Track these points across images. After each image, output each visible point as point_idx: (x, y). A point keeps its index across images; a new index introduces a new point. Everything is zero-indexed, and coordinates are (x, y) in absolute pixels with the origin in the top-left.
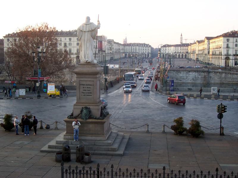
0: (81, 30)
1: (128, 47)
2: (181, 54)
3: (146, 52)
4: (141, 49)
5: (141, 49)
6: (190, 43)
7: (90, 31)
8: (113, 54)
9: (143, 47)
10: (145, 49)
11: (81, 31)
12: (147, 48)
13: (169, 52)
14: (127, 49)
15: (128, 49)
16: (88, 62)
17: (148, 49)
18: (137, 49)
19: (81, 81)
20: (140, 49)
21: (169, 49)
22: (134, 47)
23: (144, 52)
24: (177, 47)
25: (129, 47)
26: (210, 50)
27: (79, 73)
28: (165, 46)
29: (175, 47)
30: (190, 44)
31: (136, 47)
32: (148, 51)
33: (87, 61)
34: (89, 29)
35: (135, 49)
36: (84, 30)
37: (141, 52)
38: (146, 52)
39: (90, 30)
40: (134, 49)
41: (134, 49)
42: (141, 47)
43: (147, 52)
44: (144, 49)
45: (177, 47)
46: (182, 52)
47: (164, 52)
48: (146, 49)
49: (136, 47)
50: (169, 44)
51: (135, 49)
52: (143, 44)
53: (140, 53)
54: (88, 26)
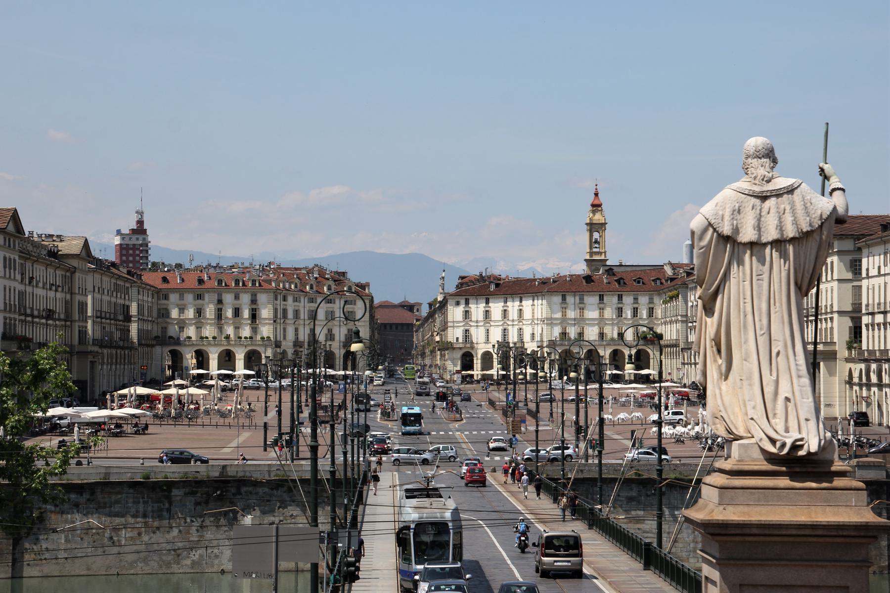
0: (726, 230)
2: (605, 353)
3: (330, 336)
4: (296, 313)
5: (296, 313)
6: (674, 266)
7: (792, 240)
8: (83, 354)
9: (312, 300)
10: (321, 315)
11: (725, 239)
12: (337, 307)
13: (513, 338)
16: (802, 453)
19: (755, 586)
20: (285, 311)
21: (513, 313)
22: (237, 297)
24: (570, 299)
26: (865, 320)
27: (747, 531)
28: (481, 287)
29: (557, 299)
30: (669, 271)
33: (795, 447)
34: (781, 228)
36: (747, 235)
37: (291, 336)
38: (330, 336)
39: (790, 232)
42: (290, 299)
43: (340, 333)
44: (313, 316)
45: (570, 299)
46: (612, 332)
47: (478, 335)
48: (330, 316)
50: (504, 269)
52: (310, 271)
53: (288, 346)
54: (772, 202)
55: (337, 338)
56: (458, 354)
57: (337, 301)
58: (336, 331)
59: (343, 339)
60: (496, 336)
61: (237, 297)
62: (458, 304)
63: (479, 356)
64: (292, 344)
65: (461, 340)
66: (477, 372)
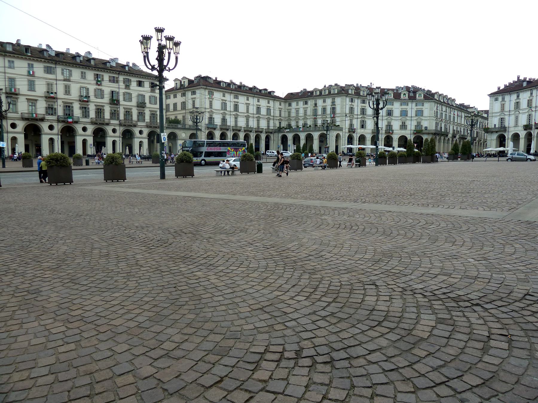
1: (301, 103)
10: (397, 113)
14: (297, 111)
15: (301, 112)
17: (419, 113)
18: (338, 110)
22: (324, 101)
23: (396, 125)
25: (306, 103)
31: (333, 103)
32: (419, 124)
35: (328, 111)
38: (403, 126)
40: (324, 109)
41: (324, 109)
43: (411, 125)
47: (510, 122)
49: (333, 103)
51: (328, 111)
55: (409, 127)
56: (495, 136)
57: (410, 104)
58: (408, 123)
59: (413, 128)
60: (523, 120)
61: (324, 101)
62: (496, 100)
63: (510, 137)
64: (371, 131)
65: (497, 126)
66: (509, 147)
